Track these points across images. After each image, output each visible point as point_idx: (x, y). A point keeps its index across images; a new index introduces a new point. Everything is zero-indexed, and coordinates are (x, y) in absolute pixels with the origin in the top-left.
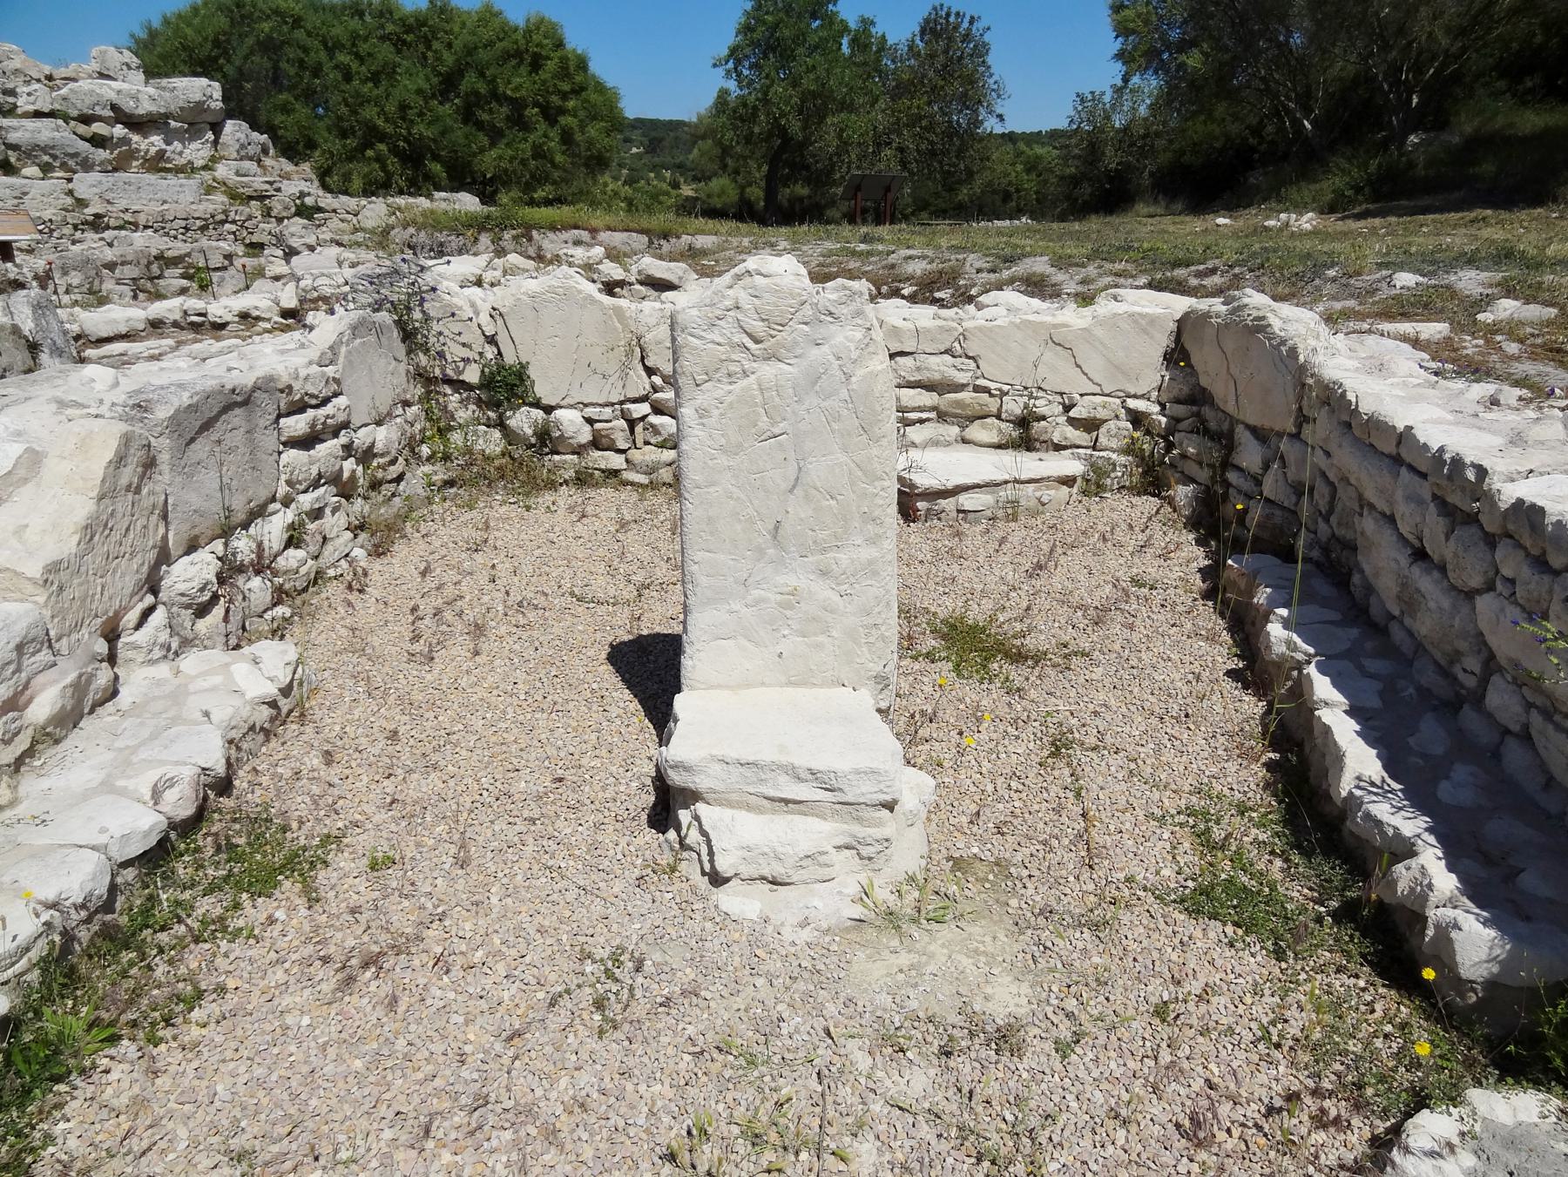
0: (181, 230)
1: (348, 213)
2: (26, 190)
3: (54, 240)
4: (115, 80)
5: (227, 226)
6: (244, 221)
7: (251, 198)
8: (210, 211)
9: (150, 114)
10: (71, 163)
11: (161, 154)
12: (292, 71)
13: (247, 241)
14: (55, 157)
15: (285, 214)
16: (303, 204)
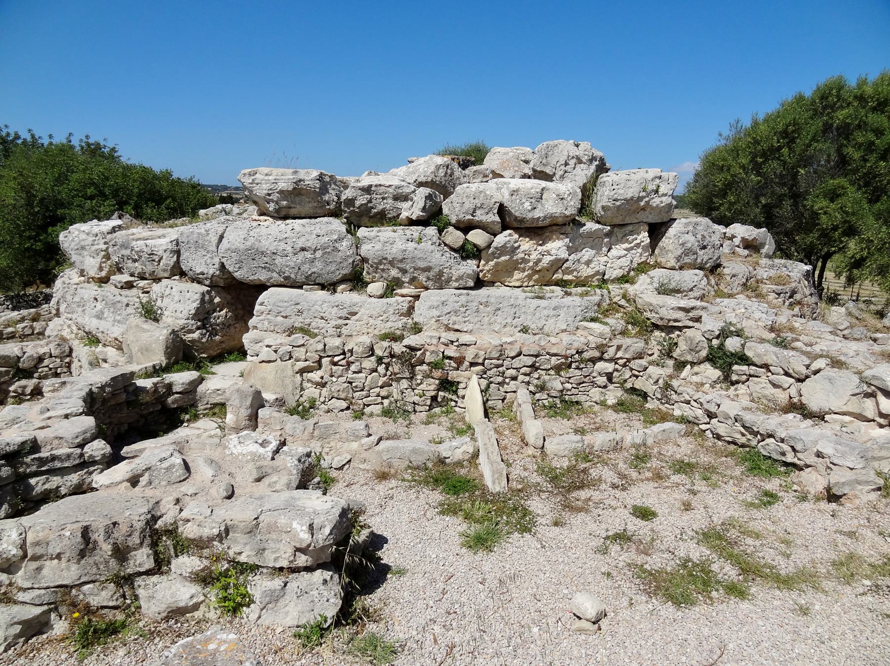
0: (527, 370)
1: (787, 374)
2: (356, 309)
3: (350, 375)
4: (502, 176)
5: (601, 366)
6: (629, 360)
7: (656, 327)
8: (576, 345)
9: (552, 216)
10: (422, 278)
11: (558, 264)
12: (857, 156)
13: (628, 385)
14: (404, 271)
15: (689, 358)
16: (721, 346)
